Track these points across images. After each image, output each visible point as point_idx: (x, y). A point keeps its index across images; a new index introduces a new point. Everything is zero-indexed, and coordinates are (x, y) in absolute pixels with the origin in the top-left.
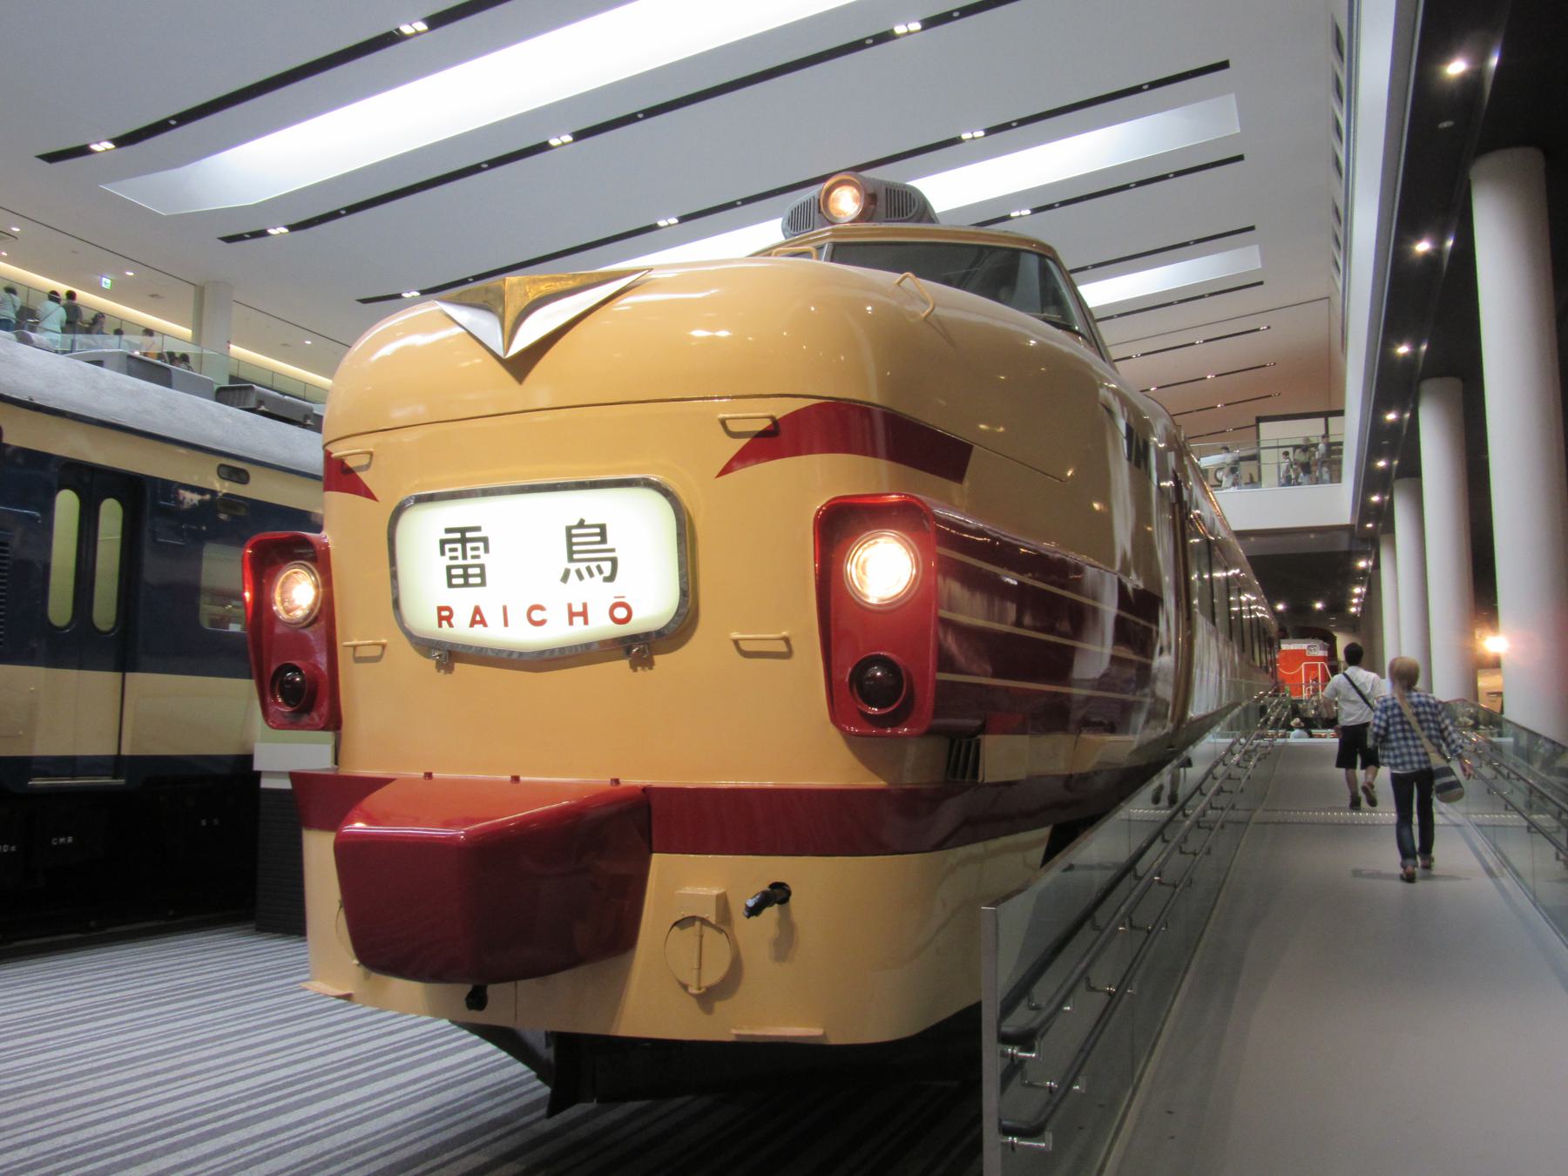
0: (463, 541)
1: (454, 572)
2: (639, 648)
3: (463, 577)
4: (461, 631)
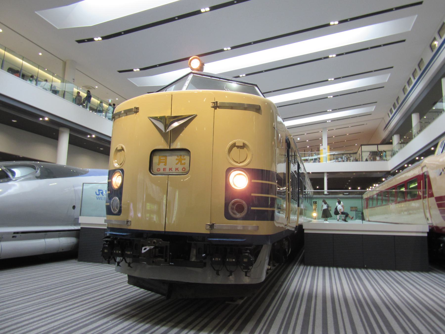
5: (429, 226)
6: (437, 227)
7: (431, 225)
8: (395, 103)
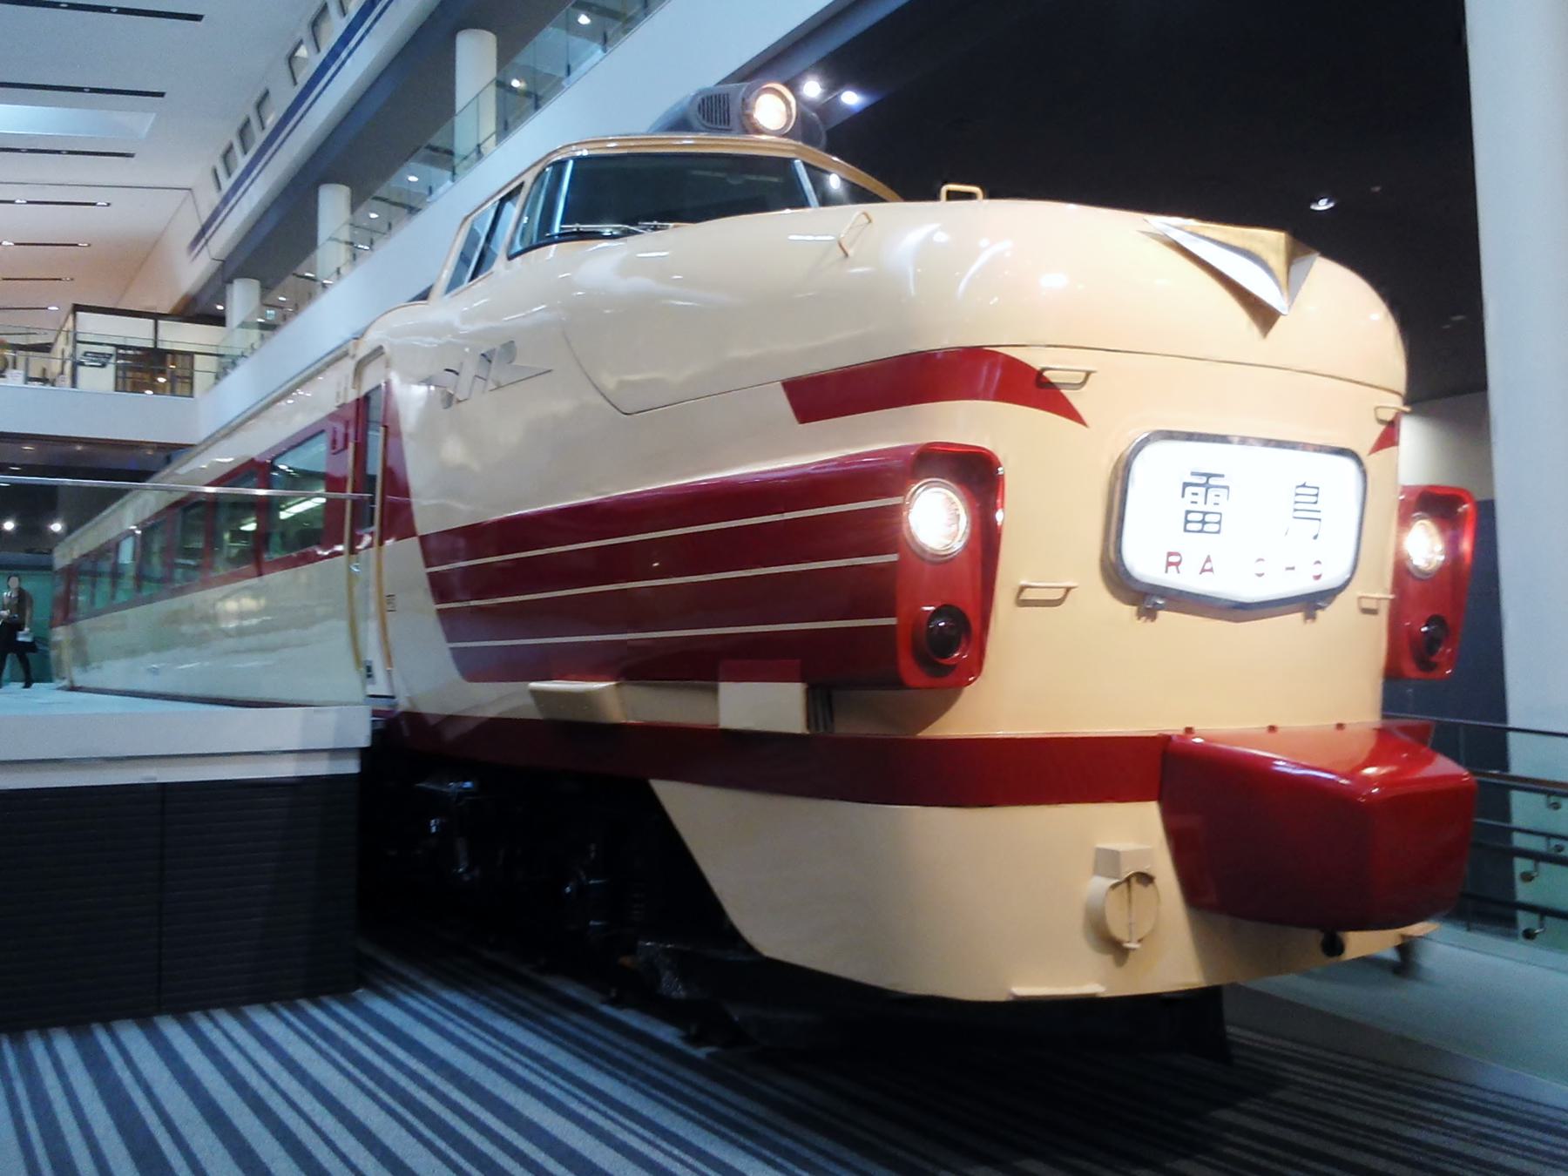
0: (1207, 486)
1: (1191, 517)
2: (1311, 603)
3: (1199, 523)
4: (1187, 580)
5: (375, 713)
6: (414, 719)
7: (382, 705)
8: (247, 123)
